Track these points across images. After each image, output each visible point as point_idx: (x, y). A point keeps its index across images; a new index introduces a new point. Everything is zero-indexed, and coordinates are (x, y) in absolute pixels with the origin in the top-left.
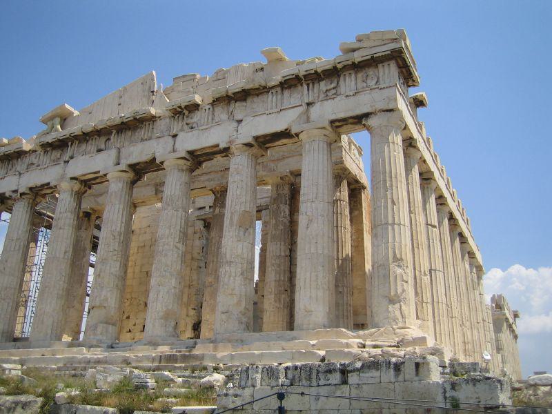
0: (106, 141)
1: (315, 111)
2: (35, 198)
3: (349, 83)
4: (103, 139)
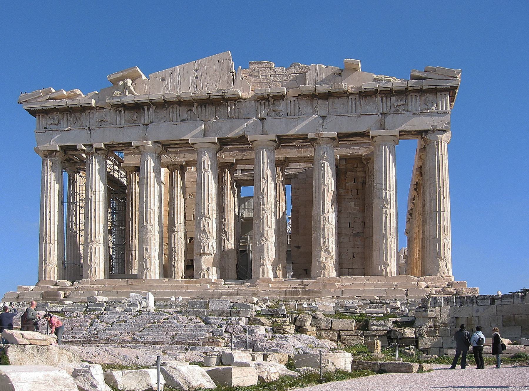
4: (184, 109)
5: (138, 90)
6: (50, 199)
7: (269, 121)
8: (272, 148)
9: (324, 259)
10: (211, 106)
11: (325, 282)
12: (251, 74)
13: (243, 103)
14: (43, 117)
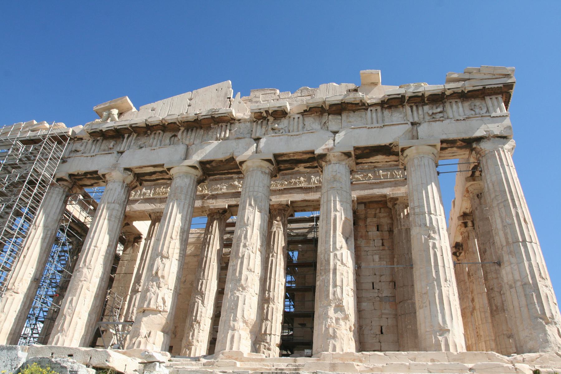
0: (172, 136)
1: (423, 130)
2: (72, 187)
3: (457, 109)
4: (169, 134)
9: (334, 321)
10: (198, 130)
11: (336, 361)
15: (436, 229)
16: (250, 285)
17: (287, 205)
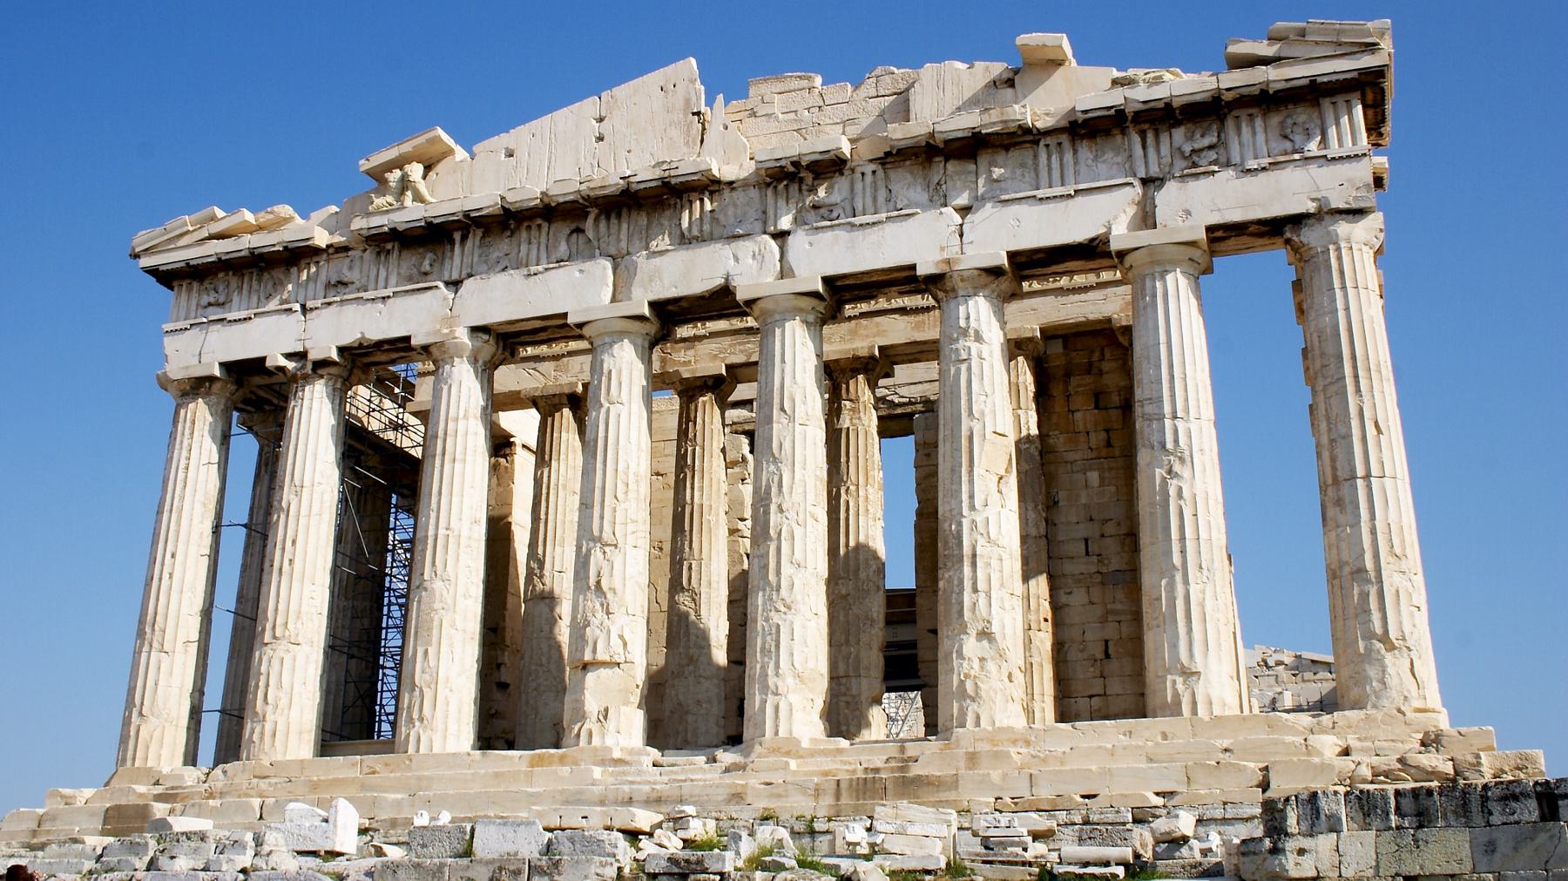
3: (1252, 138)
4: (562, 229)
5: (444, 193)
6: (180, 517)
7: (799, 242)
8: (811, 318)
9: (976, 664)
10: (634, 214)
12: (753, 114)
13: (726, 193)
14: (190, 290)
15: (1187, 453)
16: (799, 598)
17: (872, 357)
